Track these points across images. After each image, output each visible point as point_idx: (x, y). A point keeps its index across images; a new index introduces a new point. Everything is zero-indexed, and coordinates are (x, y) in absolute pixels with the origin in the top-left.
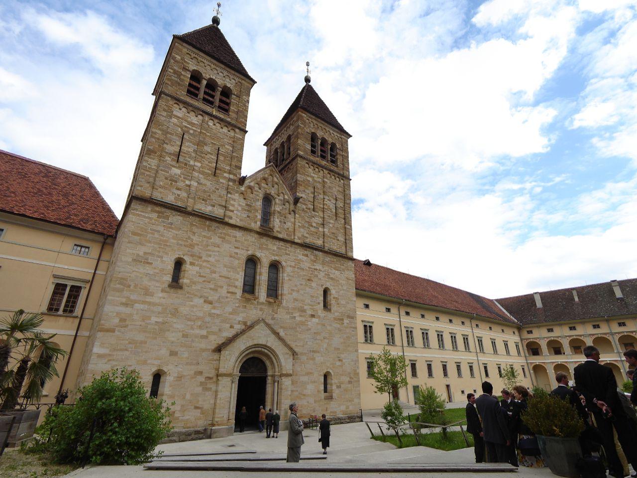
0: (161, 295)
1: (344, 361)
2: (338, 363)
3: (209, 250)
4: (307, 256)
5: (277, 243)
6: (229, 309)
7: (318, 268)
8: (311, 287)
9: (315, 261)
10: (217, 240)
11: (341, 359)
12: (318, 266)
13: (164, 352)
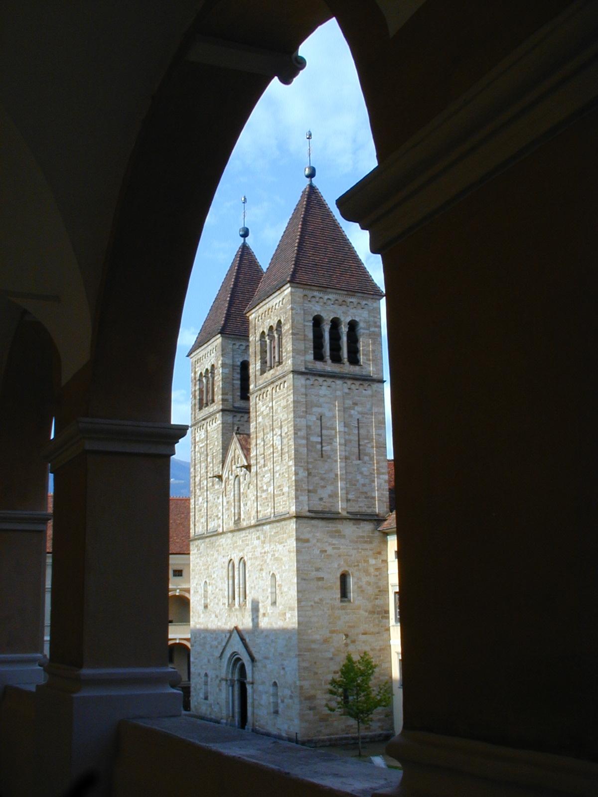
0: (202, 616)
1: (286, 669)
2: (282, 672)
3: (214, 568)
4: (258, 538)
5: (243, 534)
6: (224, 621)
7: (266, 549)
9: (264, 542)
11: (284, 666)
13: (205, 661)
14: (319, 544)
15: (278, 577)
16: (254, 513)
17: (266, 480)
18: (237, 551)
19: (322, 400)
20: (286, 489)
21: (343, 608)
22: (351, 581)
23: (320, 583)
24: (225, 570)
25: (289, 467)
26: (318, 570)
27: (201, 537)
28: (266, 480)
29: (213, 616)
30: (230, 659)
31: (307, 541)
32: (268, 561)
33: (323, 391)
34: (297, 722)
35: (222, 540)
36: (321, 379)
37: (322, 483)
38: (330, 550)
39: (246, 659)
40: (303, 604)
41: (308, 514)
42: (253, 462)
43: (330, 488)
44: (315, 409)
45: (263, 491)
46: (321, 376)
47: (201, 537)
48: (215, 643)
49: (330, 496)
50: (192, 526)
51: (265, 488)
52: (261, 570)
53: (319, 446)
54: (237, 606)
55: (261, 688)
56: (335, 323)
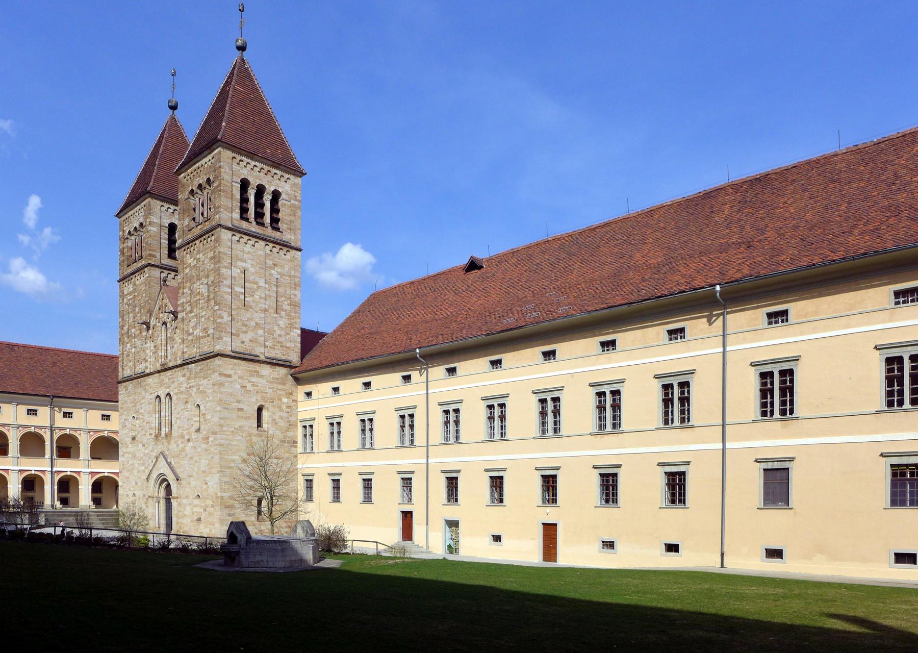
2: (205, 487)
4: (184, 375)
5: (169, 373)
8: (186, 409)
9: (189, 379)
10: (143, 393)
12: (192, 382)
14: (240, 381)
15: (202, 407)
16: (180, 354)
17: (192, 324)
18: (163, 388)
19: (246, 256)
20: (211, 331)
21: (260, 436)
22: (265, 413)
23: (240, 413)
24: (151, 406)
25: (215, 311)
26: (238, 402)
27: (130, 379)
28: (192, 324)
29: (140, 445)
30: (156, 481)
31: (230, 376)
32: (193, 394)
33: (248, 248)
34: (217, 525)
35: (150, 380)
36: (246, 237)
37: (244, 329)
38: (249, 387)
39: (171, 478)
40: (225, 429)
41: (231, 353)
42: (179, 309)
43: (250, 335)
44: (239, 263)
45: (189, 334)
46: (246, 234)
47: (130, 379)
48: (142, 468)
49: (250, 341)
50: (120, 369)
51: (191, 331)
52: (187, 402)
53: (242, 297)
54: (163, 435)
55: (185, 501)
56: (260, 190)
